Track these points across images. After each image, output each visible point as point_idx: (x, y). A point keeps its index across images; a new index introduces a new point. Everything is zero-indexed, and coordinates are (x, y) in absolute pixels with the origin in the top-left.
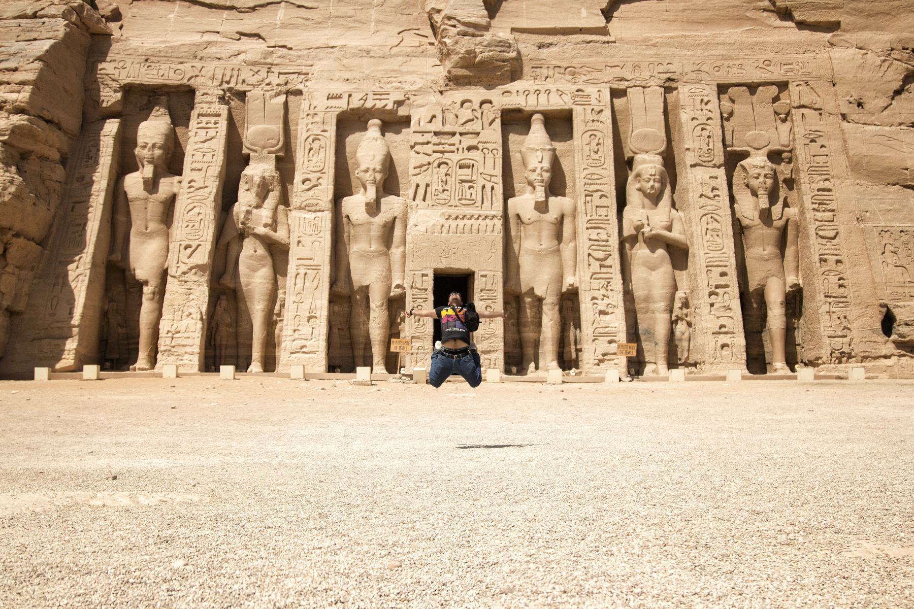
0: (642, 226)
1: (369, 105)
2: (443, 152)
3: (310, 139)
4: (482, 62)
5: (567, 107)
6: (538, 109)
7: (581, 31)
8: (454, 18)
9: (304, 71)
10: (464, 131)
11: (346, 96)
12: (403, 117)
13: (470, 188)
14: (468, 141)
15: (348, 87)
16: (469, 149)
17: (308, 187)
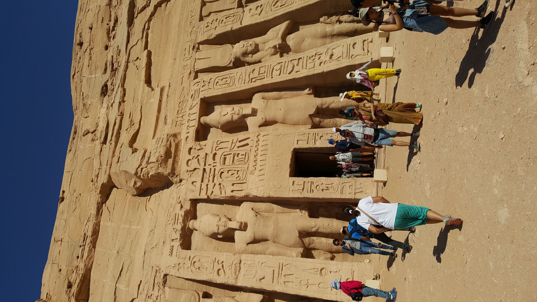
0: (275, 47)
1: (179, 227)
2: (214, 177)
3: (193, 269)
4: (166, 153)
5: (199, 102)
6: (197, 119)
7: (160, 101)
8: (137, 169)
9: (155, 273)
10: (204, 163)
11: (173, 243)
12: (191, 205)
13: (238, 156)
14: (210, 160)
15: (168, 241)
16: (214, 159)
17: (223, 272)
